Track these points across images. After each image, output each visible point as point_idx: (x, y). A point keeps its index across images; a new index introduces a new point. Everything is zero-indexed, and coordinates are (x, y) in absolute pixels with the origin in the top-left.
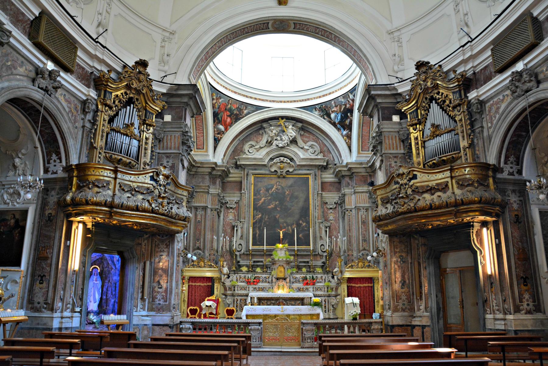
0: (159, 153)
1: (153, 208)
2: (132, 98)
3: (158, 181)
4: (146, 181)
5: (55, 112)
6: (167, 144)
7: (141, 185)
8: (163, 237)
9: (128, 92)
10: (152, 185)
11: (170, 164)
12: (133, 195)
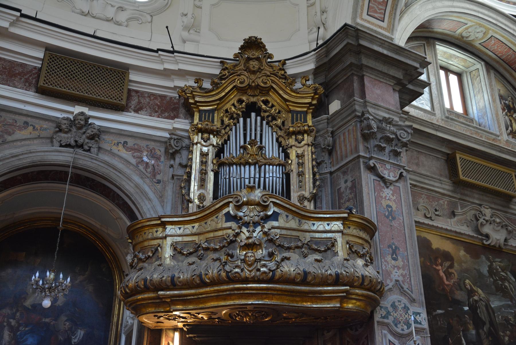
0: (331, 173)
1: (227, 272)
2: (254, 104)
3: (241, 218)
4: (219, 226)
5: (107, 171)
6: (341, 152)
7: (211, 235)
8: (357, 330)
9: (244, 98)
10: (230, 228)
11: (349, 184)
12: (201, 258)
